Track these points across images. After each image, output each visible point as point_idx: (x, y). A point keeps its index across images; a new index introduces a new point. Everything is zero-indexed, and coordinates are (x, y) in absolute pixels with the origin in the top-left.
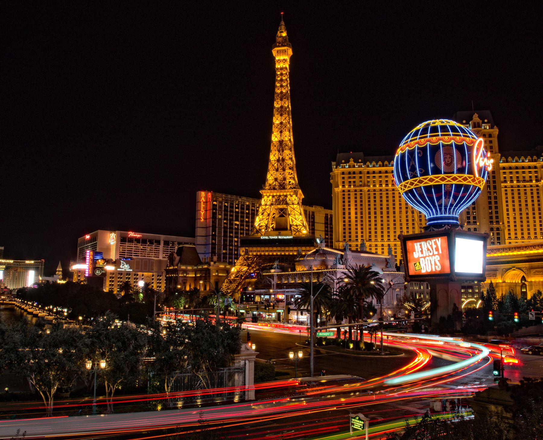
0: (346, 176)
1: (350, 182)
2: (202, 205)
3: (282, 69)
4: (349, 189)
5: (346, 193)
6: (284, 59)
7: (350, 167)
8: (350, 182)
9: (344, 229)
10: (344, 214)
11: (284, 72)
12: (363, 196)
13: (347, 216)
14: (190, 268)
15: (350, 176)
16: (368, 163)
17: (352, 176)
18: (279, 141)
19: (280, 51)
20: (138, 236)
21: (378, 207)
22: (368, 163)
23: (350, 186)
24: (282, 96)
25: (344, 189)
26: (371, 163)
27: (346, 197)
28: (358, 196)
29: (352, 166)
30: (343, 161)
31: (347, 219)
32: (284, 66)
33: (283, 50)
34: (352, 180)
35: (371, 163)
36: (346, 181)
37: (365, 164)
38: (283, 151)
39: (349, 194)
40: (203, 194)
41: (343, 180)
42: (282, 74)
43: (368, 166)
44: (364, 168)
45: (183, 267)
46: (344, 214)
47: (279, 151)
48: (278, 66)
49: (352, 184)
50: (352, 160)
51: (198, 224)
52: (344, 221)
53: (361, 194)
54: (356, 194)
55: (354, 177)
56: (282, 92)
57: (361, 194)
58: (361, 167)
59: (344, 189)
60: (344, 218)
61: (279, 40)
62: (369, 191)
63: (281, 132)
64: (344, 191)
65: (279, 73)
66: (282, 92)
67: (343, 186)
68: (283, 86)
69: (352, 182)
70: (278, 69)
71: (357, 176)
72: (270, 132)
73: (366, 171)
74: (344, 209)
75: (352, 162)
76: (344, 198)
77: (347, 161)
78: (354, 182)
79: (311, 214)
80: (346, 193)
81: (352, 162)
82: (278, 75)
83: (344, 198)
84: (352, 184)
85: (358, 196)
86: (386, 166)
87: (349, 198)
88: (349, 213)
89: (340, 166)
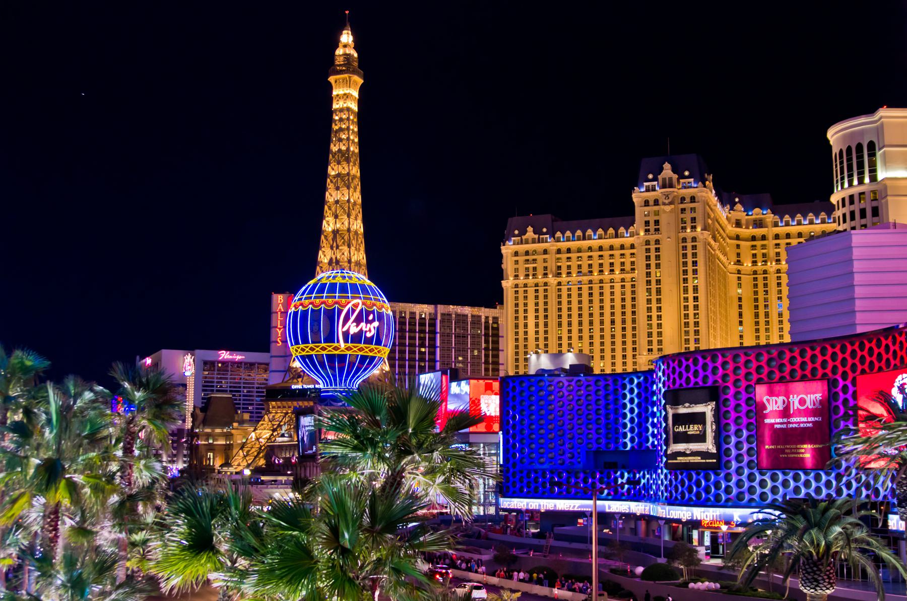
0: (521, 259)
1: (527, 269)
3: (341, 110)
4: (526, 281)
5: (521, 290)
6: (345, 94)
8: (527, 269)
9: (517, 353)
10: (517, 326)
11: (344, 117)
12: (549, 293)
13: (521, 330)
14: (218, 431)
15: (527, 257)
16: (558, 234)
17: (530, 258)
18: (333, 231)
20: (238, 357)
21: (575, 313)
22: (558, 234)
23: (527, 276)
24: (345, 156)
25: (516, 282)
26: (563, 233)
27: (521, 295)
28: (541, 294)
29: (530, 241)
30: (516, 232)
31: (521, 336)
32: (345, 105)
34: (531, 266)
35: (563, 233)
36: (522, 267)
37: (553, 235)
38: (337, 247)
39: (526, 292)
41: (516, 266)
42: (341, 120)
43: (558, 240)
44: (550, 245)
45: (208, 430)
46: (517, 326)
47: (332, 248)
48: (335, 106)
49: (531, 272)
50: (530, 229)
52: (517, 340)
53: (546, 291)
54: (537, 291)
57: (546, 291)
59: (516, 282)
60: (517, 333)
61: (339, 61)
62: (559, 284)
63: (336, 217)
64: (517, 286)
65: (337, 118)
66: (340, 150)
67: (516, 276)
68: (346, 138)
69: (531, 270)
70: (336, 110)
71: (540, 258)
72: (321, 217)
73: (555, 248)
74: (517, 318)
75: (530, 233)
76: (517, 298)
78: (535, 269)
79: (491, 322)
80: (521, 290)
81: (530, 233)
82: (335, 121)
83: (517, 298)
84: (531, 272)
85: (541, 294)
86: (590, 239)
87: (526, 298)
88: (526, 326)
89: (509, 240)
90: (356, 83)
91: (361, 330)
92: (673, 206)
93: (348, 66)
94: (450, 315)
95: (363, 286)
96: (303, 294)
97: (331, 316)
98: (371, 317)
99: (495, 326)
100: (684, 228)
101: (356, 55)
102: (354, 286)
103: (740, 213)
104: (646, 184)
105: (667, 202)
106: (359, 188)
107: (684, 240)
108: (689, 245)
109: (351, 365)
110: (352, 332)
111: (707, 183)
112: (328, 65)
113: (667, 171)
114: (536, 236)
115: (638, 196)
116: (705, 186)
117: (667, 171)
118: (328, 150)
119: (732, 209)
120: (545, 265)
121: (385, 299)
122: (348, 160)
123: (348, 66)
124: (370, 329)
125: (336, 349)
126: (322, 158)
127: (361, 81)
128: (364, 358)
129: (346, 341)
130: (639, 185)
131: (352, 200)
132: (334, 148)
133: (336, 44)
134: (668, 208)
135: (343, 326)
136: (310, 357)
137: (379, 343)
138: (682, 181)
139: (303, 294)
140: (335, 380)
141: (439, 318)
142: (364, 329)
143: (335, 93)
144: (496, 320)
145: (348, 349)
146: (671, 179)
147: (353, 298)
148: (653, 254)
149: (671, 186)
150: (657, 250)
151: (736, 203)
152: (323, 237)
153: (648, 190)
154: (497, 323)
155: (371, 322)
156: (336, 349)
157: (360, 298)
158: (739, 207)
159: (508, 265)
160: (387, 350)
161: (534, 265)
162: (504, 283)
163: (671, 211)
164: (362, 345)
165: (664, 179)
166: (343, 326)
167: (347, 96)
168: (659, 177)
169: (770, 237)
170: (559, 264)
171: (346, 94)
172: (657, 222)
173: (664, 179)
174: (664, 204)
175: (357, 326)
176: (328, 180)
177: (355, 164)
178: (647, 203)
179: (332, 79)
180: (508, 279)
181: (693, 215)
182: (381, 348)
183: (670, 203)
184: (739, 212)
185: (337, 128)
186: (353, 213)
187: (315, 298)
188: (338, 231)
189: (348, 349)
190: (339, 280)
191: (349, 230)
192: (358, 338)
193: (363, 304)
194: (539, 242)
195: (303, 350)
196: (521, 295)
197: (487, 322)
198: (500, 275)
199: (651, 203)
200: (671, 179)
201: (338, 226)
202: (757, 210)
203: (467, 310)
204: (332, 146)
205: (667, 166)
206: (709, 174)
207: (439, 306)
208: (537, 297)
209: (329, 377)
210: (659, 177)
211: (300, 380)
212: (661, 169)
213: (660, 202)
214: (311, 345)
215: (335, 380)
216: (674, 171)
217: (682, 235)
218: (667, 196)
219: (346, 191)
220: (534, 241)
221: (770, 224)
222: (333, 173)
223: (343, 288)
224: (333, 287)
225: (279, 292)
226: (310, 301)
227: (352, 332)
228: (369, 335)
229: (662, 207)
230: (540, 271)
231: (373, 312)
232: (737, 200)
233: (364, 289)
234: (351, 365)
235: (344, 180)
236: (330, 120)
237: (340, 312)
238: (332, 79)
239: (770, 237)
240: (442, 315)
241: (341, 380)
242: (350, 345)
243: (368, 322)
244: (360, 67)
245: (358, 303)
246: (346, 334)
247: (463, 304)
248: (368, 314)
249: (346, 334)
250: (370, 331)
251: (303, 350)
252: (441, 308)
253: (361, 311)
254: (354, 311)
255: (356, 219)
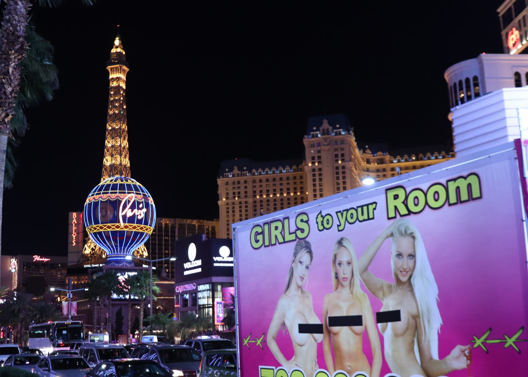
1: (234, 193)
2: (74, 228)
5: (230, 207)
6: (117, 78)
7: (233, 176)
15: (234, 186)
16: (254, 171)
18: (110, 165)
19: (114, 68)
22: (254, 171)
27: (230, 210)
28: (243, 209)
30: (227, 170)
33: (116, 68)
35: (257, 170)
37: (250, 172)
40: (75, 215)
49: (237, 195)
50: (236, 168)
51: (70, 250)
55: (239, 187)
56: (114, 113)
58: (246, 175)
61: (113, 56)
63: (112, 156)
66: (114, 113)
72: (103, 156)
75: (236, 171)
77: (231, 170)
84: (237, 195)
85: (243, 209)
90: (124, 70)
91: (134, 214)
92: (329, 147)
93: (120, 59)
94: (184, 225)
95: (135, 186)
96: (95, 192)
97: (115, 204)
98: (141, 206)
99: (213, 231)
100: (337, 161)
101: (124, 53)
102: (129, 186)
103: (369, 155)
104: (312, 133)
105: (326, 144)
106: (127, 138)
107: (337, 168)
108: (340, 171)
109: (128, 238)
110: (128, 216)
111: (351, 132)
112: (106, 58)
113: (326, 125)
114: (240, 172)
115: (307, 141)
116: (349, 134)
117: (326, 125)
118: (106, 113)
119: (364, 152)
120: (246, 190)
121: (149, 195)
122: (120, 120)
123: (120, 59)
124: (141, 214)
125: (118, 227)
126: (103, 119)
127: (127, 69)
128: (136, 233)
129: (124, 222)
130: (308, 134)
131: (123, 146)
132: (111, 112)
133: (112, 45)
134: (326, 148)
135: (123, 210)
136: (100, 233)
137: (146, 223)
138: (335, 131)
139: (95, 192)
140: (117, 249)
141: (177, 226)
142: (136, 214)
143: (111, 77)
144: (213, 228)
145: (126, 227)
146: (328, 129)
147: (129, 193)
148: (317, 177)
149: (328, 134)
150: (320, 175)
151: (366, 149)
152: (103, 169)
153: (313, 137)
154: (214, 230)
155: (141, 209)
156: (118, 227)
157: (133, 193)
158: (368, 151)
159: (221, 191)
160: (152, 228)
161: (239, 191)
162: (220, 203)
163: (328, 150)
164: (135, 225)
165: (323, 130)
166: (123, 210)
167: (118, 79)
168: (321, 128)
169: (388, 169)
170: (255, 190)
171: (118, 77)
172: (319, 157)
173: (323, 130)
174: (324, 145)
175: (132, 211)
176: (107, 133)
177: (124, 123)
178: (313, 146)
179: (109, 68)
180: (222, 200)
181: (342, 152)
182: (148, 227)
183: (328, 145)
184: (369, 155)
185: (112, 99)
186: (124, 153)
187: (103, 193)
188: (114, 164)
189: (126, 227)
190: (119, 182)
191: (121, 164)
192: (132, 219)
193: (136, 197)
194: (241, 176)
195: (95, 229)
196: (230, 210)
197: (208, 229)
198: (217, 198)
199: (316, 145)
200: (328, 129)
201: (113, 162)
202: (380, 153)
203: (195, 222)
204: (109, 111)
205: (325, 122)
206: (351, 127)
207: (177, 219)
208: (241, 211)
209: (112, 247)
210: (321, 128)
211: (89, 262)
212: (322, 123)
213: (321, 144)
214: (100, 225)
215: (117, 249)
216: (330, 124)
217: (336, 165)
218: (326, 140)
219: (118, 140)
220: (238, 175)
221: (388, 162)
222: (110, 128)
223: (122, 187)
224: (114, 187)
225: (75, 212)
226: (100, 196)
227: (128, 216)
228: (140, 217)
229: (323, 147)
230: (242, 194)
231: (142, 202)
232: (367, 147)
233: (136, 189)
234: (128, 238)
235: (116, 133)
236: (108, 95)
237: (121, 202)
238: (109, 68)
239: (388, 169)
240: (179, 225)
241: (121, 249)
242: (127, 224)
243: (139, 209)
244: (126, 59)
245: (133, 196)
246: (124, 217)
247: (193, 218)
248: (139, 203)
249: (124, 217)
250: (140, 215)
251: (95, 229)
252: (178, 221)
253: (134, 201)
254: (129, 202)
255: (125, 158)
